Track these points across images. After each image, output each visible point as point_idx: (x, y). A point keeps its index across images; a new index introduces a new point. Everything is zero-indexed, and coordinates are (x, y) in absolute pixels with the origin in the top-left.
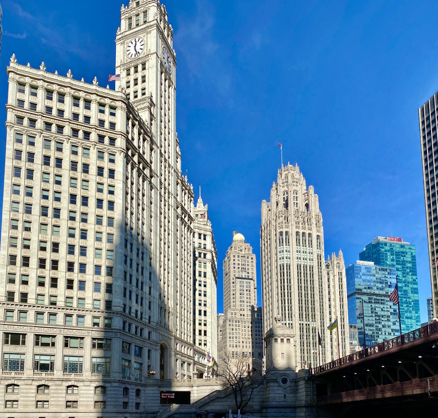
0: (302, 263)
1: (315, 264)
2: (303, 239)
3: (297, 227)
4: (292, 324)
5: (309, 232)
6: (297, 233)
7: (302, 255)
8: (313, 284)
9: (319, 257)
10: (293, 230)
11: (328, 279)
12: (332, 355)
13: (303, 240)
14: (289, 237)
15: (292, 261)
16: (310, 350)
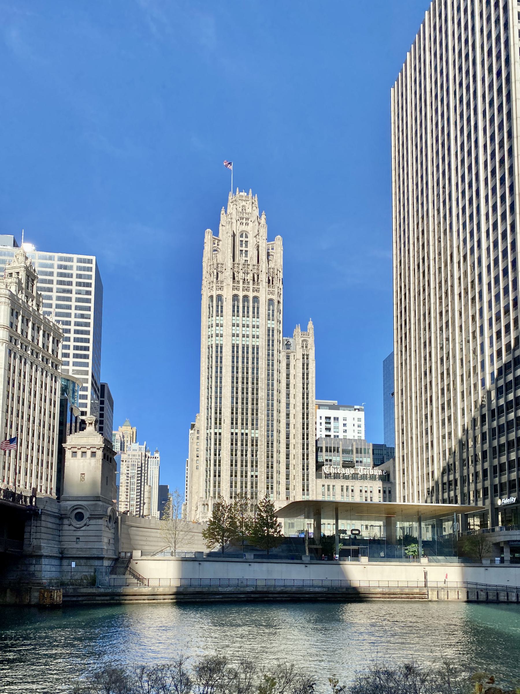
0: (239, 341)
1: (262, 343)
2: (244, 306)
3: (234, 288)
4: (220, 434)
5: (255, 294)
6: (235, 297)
7: (239, 330)
8: (257, 373)
9: (270, 331)
10: (227, 294)
11: (288, 365)
12: (287, 479)
13: (244, 307)
14: (222, 303)
15: (225, 340)
16: (246, 473)
